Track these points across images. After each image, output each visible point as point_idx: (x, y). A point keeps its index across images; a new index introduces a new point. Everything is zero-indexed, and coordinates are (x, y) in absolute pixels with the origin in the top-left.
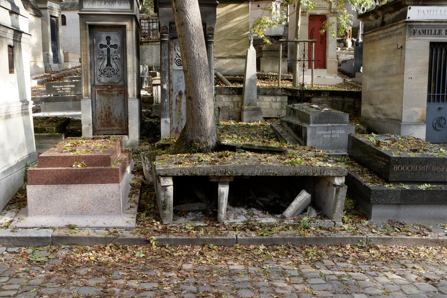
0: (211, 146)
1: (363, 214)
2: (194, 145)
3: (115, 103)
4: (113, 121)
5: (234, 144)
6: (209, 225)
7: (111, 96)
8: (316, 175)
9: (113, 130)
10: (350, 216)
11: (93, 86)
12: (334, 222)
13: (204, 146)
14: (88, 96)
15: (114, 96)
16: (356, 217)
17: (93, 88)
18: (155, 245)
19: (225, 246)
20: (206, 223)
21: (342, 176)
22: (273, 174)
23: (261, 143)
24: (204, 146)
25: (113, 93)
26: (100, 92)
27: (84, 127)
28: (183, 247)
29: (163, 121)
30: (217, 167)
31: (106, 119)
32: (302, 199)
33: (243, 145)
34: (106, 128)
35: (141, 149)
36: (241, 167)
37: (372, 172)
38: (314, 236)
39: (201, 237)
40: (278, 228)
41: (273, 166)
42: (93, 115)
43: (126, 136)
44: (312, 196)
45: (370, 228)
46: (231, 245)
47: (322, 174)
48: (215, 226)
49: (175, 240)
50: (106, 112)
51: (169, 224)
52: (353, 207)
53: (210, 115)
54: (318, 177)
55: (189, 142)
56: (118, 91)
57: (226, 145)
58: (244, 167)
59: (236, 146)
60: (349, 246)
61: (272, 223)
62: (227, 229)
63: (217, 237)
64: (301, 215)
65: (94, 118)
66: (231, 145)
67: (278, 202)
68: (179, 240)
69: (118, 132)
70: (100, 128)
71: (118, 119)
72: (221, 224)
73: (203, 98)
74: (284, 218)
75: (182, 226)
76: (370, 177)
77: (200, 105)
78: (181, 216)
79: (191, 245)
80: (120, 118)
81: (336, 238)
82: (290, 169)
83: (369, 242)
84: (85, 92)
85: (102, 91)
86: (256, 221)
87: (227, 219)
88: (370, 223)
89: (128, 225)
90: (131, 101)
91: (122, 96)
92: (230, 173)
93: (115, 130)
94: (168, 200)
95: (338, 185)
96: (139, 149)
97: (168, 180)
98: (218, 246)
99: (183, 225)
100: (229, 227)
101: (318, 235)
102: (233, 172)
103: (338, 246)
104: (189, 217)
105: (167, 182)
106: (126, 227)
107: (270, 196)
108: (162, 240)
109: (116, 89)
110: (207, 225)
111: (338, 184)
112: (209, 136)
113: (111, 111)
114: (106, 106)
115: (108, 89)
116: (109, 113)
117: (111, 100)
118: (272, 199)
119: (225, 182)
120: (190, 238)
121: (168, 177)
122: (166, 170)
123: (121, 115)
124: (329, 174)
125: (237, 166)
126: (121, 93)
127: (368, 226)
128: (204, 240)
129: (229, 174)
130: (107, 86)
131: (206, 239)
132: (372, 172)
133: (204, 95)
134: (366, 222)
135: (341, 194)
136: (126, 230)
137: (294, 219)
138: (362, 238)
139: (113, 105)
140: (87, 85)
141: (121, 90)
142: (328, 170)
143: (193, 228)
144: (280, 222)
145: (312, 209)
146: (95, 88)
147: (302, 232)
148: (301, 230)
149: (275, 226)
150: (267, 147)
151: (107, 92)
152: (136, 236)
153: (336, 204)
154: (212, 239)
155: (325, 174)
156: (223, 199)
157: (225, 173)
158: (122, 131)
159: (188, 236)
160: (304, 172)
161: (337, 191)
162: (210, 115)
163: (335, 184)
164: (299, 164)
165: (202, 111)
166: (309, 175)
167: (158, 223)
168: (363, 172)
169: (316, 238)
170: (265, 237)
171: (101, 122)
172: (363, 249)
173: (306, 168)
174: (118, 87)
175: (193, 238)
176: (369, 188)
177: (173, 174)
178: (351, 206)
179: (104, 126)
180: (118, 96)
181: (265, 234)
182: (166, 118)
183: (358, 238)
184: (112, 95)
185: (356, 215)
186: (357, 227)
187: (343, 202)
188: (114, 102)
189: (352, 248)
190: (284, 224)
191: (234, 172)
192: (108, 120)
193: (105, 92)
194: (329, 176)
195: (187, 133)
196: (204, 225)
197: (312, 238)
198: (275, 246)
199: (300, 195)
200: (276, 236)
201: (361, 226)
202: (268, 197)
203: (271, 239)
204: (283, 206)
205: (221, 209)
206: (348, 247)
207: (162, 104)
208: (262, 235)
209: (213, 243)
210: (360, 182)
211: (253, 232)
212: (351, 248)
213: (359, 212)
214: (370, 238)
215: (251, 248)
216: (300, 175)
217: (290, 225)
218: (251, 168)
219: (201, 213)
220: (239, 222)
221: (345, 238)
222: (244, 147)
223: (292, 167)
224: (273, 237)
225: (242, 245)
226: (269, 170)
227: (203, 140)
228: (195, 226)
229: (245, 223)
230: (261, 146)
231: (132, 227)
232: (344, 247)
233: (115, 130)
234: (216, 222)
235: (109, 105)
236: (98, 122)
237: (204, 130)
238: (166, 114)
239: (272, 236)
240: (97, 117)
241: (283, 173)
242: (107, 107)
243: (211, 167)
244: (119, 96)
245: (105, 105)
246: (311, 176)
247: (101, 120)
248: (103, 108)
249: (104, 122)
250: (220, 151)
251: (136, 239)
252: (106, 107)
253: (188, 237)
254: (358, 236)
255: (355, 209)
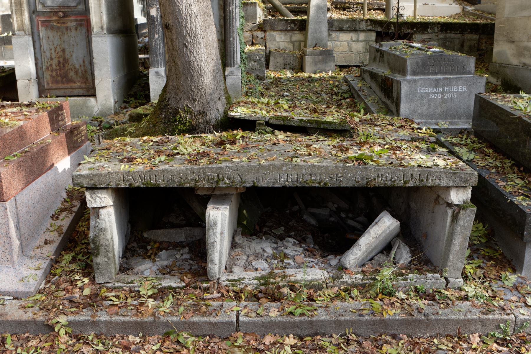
0: (214, 120)
1: (505, 257)
2: (180, 117)
3: (73, 43)
4: (72, 74)
5: (254, 116)
6: (187, 285)
7: (65, 31)
8: (410, 184)
9: (72, 88)
10: (478, 262)
11: (34, 13)
12: (446, 279)
13: (200, 121)
14: (23, 30)
15: (70, 30)
16: (491, 266)
17: (34, 16)
18: (66, 333)
19: (212, 336)
20: (183, 280)
21: (466, 187)
22: (319, 183)
23: (309, 113)
24: (200, 121)
25: (69, 24)
26: (46, 24)
27: (20, 84)
28: (123, 339)
29: (152, 72)
30: (200, 169)
31: (60, 70)
32: (380, 232)
33: (271, 118)
34: (60, 86)
35: (116, 121)
36: (251, 169)
37: (522, 169)
38: (403, 316)
39: (162, 318)
40: (329, 291)
41: (319, 167)
42: (36, 64)
43: (92, 99)
44: (400, 223)
45: (520, 293)
46: (224, 335)
47: (425, 183)
48: (200, 288)
49: (108, 323)
50: (59, 58)
51: (108, 283)
52: (483, 241)
53: (209, 59)
54: (416, 189)
55: (171, 113)
56: (76, 21)
57: (236, 119)
58: (258, 170)
59: (255, 121)
60: (478, 339)
61: (317, 280)
62: (223, 295)
63: (196, 319)
64: (379, 255)
65: (39, 69)
66: (247, 118)
67: (343, 215)
68: (117, 323)
69: (81, 92)
70: (51, 85)
71: (80, 71)
72: (212, 283)
73: (191, 27)
74: (342, 268)
75: (134, 287)
76: (520, 182)
77: (187, 40)
78: (145, 258)
79: (141, 335)
80: (82, 68)
81: (448, 320)
82: (357, 173)
83: (521, 328)
84: (18, 24)
85: (50, 21)
86: (284, 276)
87: (229, 269)
88: (520, 280)
89: (22, 288)
90: (97, 39)
91: (84, 30)
92: (227, 181)
93: (75, 88)
94: (102, 237)
95: (457, 205)
96: (112, 121)
97: (100, 195)
98: (197, 336)
99: (136, 284)
100: (228, 292)
101: (411, 315)
102: (236, 180)
103: (452, 337)
104: (162, 260)
105: (98, 200)
106: (16, 292)
107: (330, 204)
108: (81, 324)
109: (72, 18)
110: (184, 284)
111: (456, 202)
112: (209, 100)
113: (68, 56)
114: (58, 47)
115: (59, 17)
116: (64, 59)
117: (66, 37)
118: (334, 209)
119: (225, 195)
120: (139, 319)
121: (99, 191)
122: (94, 176)
123: (84, 62)
124: (438, 182)
125: (243, 167)
126: (81, 25)
127: (515, 288)
128: (166, 324)
129: (225, 183)
130: (57, 12)
131: (173, 322)
132: (522, 169)
133: (193, 20)
134: (512, 278)
135: (461, 223)
136: (15, 299)
137: (362, 271)
138: (506, 321)
139: (70, 45)
140: (21, 11)
141: (81, 20)
142: (438, 174)
143: (156, 291)
144: (334, 279)
145: (402, 245)
146: (38, 16)
147: (377, 304)
148: (375, 300)
149: (325, 286)
150: (317, 122)
151: (58, 23)
152: (29, 316)
153: (451, 244)
154: (185, 322)
155: (430, 183)
156: (215, 234)
157: (217, 182)
158: (88, 91)
159: (136, 315)
160: (384, 179)
161: (455, 217)
162: (209, 59)
163: (449, 202)
164: (375, 161)
165: (191, 52)
166: (396, 185)
167: (86, 280)
168: (504, 169)
169: (407, 320)
170: (297, 319)
171: (51, 76)
172: (507, 346)
173: (390, 171)
174: (76, 14)
175: (146, 319)
176: (521, 209)
177: (108, 185)
178: (480, 237)
179: (57, 82)
180: (76, 30)
181: (299, 311)
182: (158, 67)
183: (497, 320)
184: (67, 28)
185: (490, 259)
186: (493, 291)
187: (465, 239)
188: (71, 41)
189: (484, 343)
190: (343, 283)
191: (237, 179)
192: (62, 71)
193: (55, 24)
194: (438, 187)
195: (169, 96)
196: (179, 285)
197: (399, 320)
198: (319, 337)
199: (376, 223)
200: (321, 315)
201: (501, 289)
202: (326, 207)
203: (311, 322)
204: (353, 225)
205: (211, 255)
206: (475, 339)
207: (150, 43)
208: (291, 313)
209: (187, 331)
210: (501, 194)
211: (274, 304)
212: (482, 344)
213: (497, 251)
214: (523, 321)
215: (267, 343)
216: (377, 185)
217: (354, 285)
218: (272, 171)
219: (186, 250)
220: (250, 280)
221: (469, 321)
222: (273, 122)
223: (359, 169)
224: (315, 318)
225: (249, 335)
226: (311, 175)
227: (197, 109)
228: (159, 286)
229: (262, 281)
230: (304, 121)
231: (28, 293)
232: (465, 341)
233: (75, 88)
234: (203, 278)
235: (63, 46)
236: (47, 76)
237: (199, 90)
238: (157, 61)
239: (312, 316)
240: (44, 67)
241: (341, 181)
242: (60, 50)
243: (187, 170)
244: (78, 30)
245: (55, 46)
246: (400, 187)
247: (52, 71)
248: (53, 51)
249: (57, 75)
250: (225, 131)
251: (26, 321)
252: (58, 50)
253: (135, 318)
254: (497, 316)
255: (487, 245)
